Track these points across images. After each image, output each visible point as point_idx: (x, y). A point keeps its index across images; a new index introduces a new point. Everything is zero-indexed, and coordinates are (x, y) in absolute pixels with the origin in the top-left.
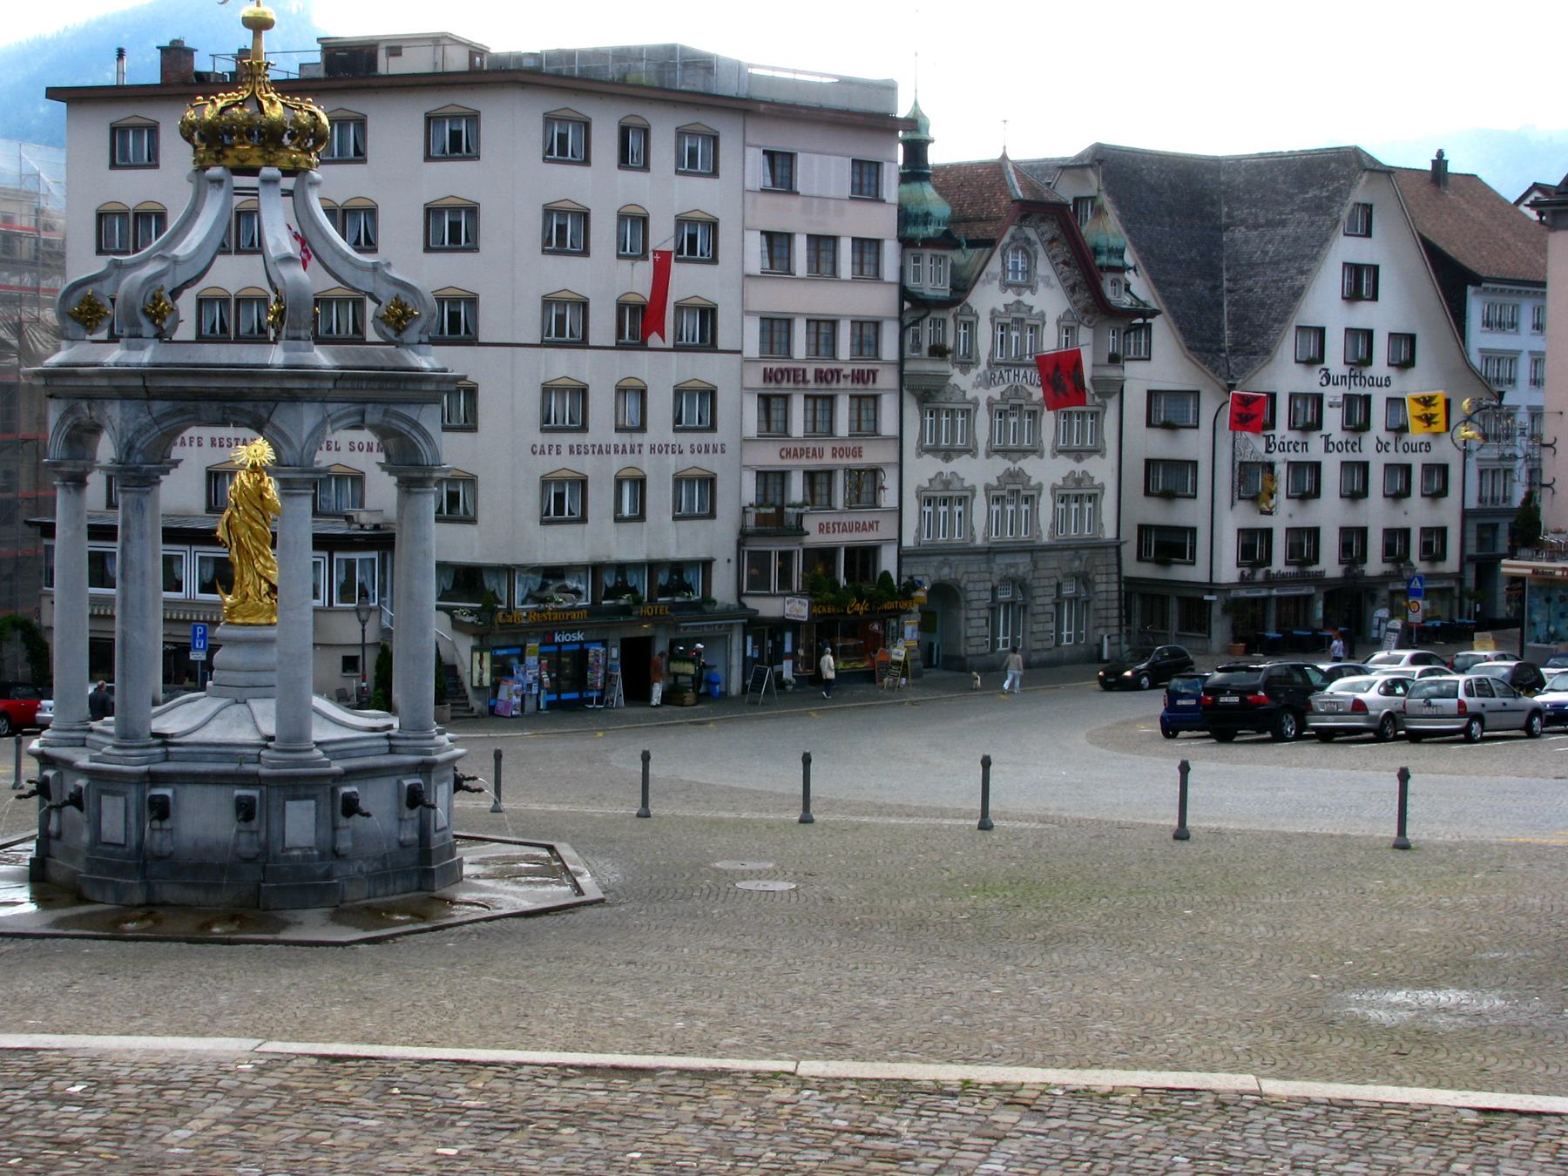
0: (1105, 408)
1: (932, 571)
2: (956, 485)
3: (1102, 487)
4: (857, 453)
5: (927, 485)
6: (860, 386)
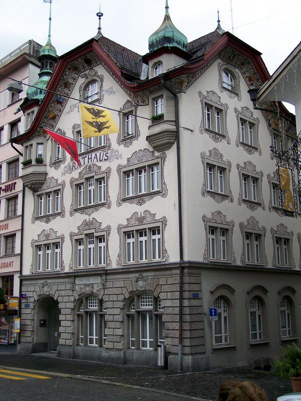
0: (164, 158)
1: (38, 289)
2: (53, 236)
3: (164, 221)
4: (6, 227)
5: (36, 238)
6: (9, 193)
